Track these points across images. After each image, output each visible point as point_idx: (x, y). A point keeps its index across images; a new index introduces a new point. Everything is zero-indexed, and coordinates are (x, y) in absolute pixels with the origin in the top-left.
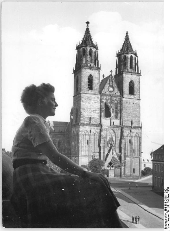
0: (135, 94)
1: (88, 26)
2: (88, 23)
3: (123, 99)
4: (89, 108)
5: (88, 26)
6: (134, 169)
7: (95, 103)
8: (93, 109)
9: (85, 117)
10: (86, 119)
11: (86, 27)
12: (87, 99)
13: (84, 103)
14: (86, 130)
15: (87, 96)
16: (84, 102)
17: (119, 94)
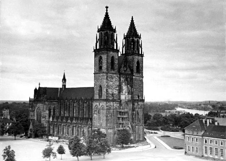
0: (140, 72)
1: (107, 10)
2: (107, 7)
3: (134, 77)
4: (112, 85)
5: (107, 10)
6: (140, 135)
7: (116, 81)
8: (115, 86)
9: (109, 93)
10: (110, 95)
11: (106, 12)
12: (111, 78)
13: (109, 82)
14: (110, 105)
15: (111, 75)
16: (109, 81)
17: (130, 73)
